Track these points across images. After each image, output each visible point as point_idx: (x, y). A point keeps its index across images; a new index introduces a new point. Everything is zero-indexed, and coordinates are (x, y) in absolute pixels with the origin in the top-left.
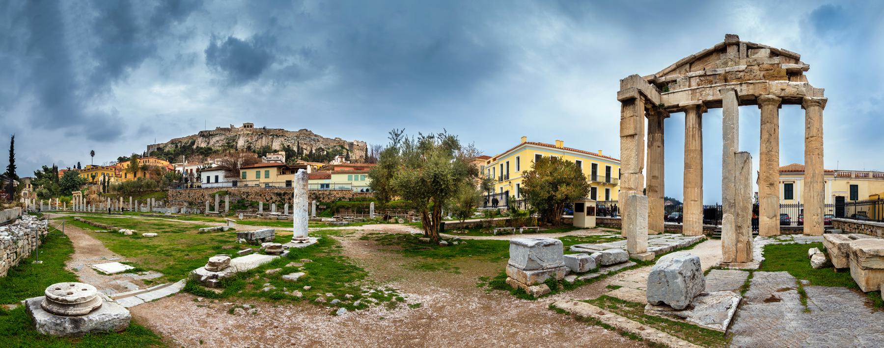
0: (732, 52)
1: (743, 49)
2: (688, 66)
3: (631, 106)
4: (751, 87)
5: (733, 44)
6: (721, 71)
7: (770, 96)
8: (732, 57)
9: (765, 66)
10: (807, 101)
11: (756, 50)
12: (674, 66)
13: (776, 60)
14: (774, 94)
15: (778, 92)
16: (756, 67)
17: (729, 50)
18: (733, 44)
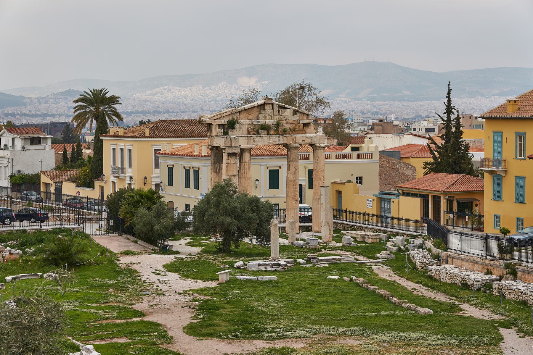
0: (268, 108)
1: (276, 108)
2: (238, 114)
3: (234, 157)
4: (285, 138)
5: (269, 104)
6: (262, 122)
7: (297, 145)
8: (269, 113)
9: (290, 121)
10: (316, 146)
11: (285, 110)
12: (230, 113)
13: (296, 118)
14: (298, 144)
15: (301, 142)
16: (284, 122)
17: (267, 107)
18: (269, 104)
